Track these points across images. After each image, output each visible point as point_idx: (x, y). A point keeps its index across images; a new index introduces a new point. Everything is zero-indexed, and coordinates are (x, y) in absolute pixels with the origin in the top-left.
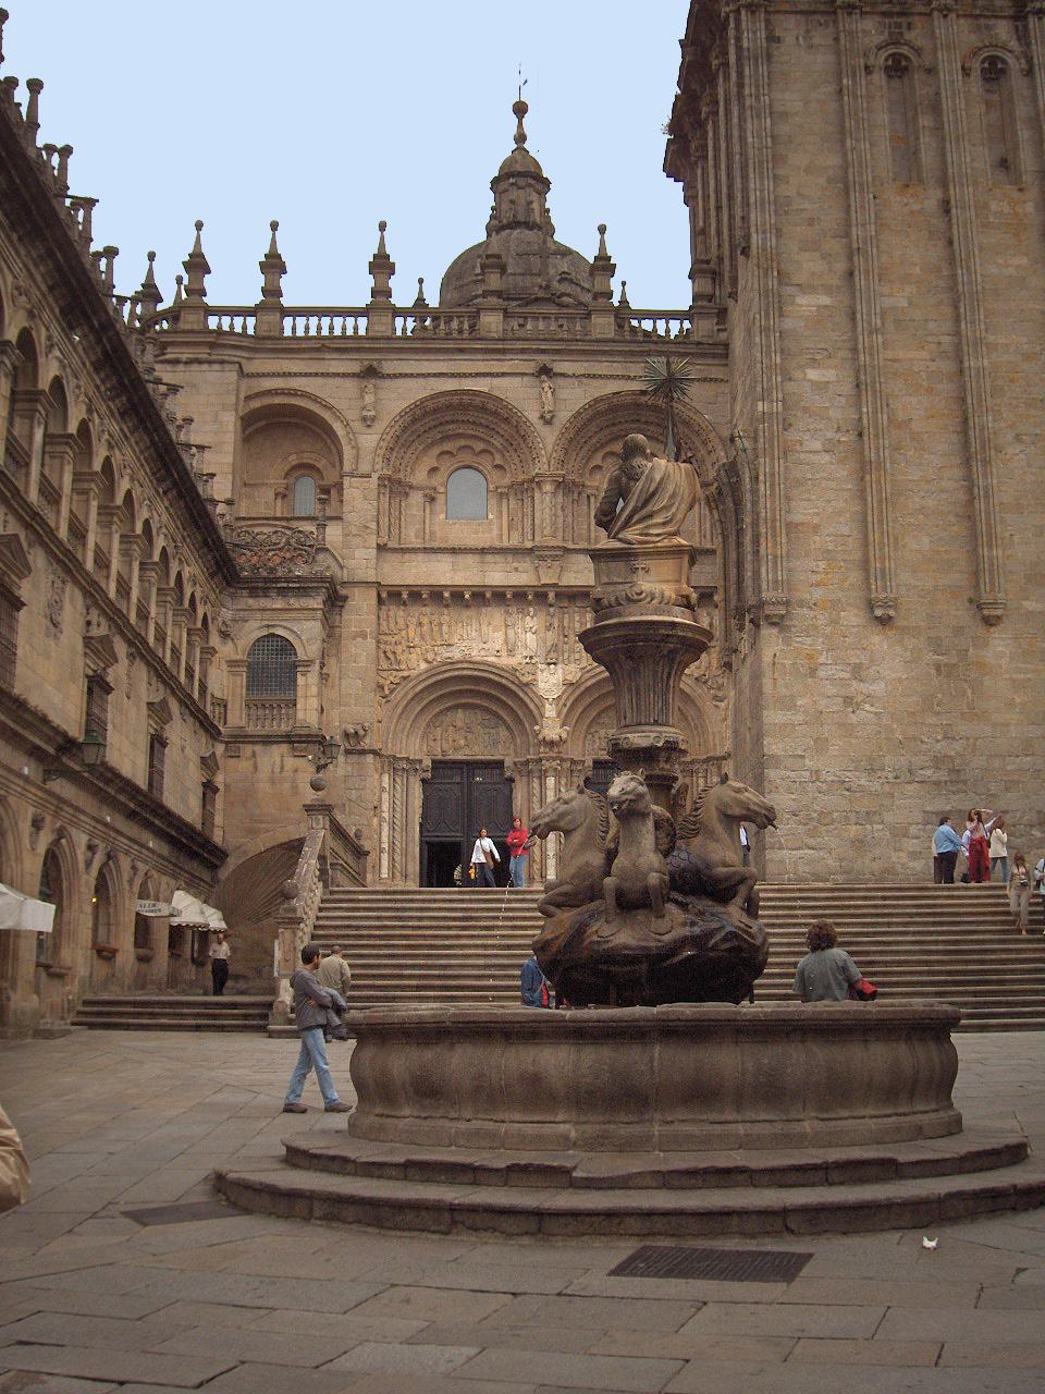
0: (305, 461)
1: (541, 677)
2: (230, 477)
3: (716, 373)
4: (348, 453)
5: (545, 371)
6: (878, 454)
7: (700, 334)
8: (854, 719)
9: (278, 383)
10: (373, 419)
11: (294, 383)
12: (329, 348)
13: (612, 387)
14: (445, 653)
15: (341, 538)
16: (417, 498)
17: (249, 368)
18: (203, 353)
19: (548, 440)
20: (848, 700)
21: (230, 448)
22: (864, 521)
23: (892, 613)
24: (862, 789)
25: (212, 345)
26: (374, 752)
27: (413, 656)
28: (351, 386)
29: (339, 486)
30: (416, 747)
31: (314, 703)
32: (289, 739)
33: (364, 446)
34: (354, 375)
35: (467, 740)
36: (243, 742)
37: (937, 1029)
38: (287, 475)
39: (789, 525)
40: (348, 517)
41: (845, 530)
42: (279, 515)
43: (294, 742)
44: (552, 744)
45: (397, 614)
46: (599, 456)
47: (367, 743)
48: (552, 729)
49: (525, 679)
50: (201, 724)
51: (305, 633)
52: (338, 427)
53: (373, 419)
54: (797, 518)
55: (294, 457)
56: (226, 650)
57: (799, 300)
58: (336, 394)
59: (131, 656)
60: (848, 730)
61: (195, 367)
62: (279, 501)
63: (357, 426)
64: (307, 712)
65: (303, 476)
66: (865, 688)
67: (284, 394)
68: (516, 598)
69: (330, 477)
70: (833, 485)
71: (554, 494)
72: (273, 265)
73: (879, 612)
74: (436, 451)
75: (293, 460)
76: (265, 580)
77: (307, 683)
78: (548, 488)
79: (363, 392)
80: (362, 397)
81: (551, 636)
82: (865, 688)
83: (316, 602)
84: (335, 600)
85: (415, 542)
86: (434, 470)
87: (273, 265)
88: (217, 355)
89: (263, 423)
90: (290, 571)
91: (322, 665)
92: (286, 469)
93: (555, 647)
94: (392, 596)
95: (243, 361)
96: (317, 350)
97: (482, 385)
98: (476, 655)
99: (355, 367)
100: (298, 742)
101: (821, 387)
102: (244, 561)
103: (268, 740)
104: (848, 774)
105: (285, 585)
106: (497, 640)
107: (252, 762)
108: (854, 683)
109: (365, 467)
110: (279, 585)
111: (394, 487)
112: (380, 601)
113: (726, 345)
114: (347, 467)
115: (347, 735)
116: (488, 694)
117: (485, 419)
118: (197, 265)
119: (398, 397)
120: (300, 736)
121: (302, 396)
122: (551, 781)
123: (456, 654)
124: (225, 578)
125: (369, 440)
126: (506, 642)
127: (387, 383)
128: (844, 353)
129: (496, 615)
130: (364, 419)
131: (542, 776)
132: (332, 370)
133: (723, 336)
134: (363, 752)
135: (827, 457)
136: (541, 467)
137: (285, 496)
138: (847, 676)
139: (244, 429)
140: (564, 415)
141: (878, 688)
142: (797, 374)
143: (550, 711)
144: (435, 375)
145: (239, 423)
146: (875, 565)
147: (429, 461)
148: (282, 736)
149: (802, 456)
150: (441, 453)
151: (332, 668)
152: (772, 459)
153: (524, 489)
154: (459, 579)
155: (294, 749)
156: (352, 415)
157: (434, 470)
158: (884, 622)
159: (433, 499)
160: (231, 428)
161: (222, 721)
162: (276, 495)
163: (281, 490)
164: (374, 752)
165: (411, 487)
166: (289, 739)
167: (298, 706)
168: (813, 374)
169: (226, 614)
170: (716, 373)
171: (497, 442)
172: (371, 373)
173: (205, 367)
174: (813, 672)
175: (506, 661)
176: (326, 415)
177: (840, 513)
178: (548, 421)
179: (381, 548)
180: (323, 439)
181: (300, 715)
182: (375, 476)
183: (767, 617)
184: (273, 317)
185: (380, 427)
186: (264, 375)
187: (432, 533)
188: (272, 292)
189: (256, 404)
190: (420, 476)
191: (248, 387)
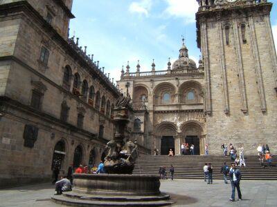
19: (177, 89)
30: (161, 134)
35: (167, 133)
45: (156, 115)
48: (179, 131)
51: (142, 118)
58: (148, 84)
59: (110, 122)
68: (173, 112)
72: (138, 66)
83: (144, 114)
84: (146, 113)
87: (138, 66)
94: (155, 112)
111: (156, 97)
116: (171, 126)
119: (157, 83)
125: (152, 90)
129: (171, 114)
136: (176, 92)
151: (147, 123)
153: (174, 96)
188: (138, 70)
190: (160, 95)
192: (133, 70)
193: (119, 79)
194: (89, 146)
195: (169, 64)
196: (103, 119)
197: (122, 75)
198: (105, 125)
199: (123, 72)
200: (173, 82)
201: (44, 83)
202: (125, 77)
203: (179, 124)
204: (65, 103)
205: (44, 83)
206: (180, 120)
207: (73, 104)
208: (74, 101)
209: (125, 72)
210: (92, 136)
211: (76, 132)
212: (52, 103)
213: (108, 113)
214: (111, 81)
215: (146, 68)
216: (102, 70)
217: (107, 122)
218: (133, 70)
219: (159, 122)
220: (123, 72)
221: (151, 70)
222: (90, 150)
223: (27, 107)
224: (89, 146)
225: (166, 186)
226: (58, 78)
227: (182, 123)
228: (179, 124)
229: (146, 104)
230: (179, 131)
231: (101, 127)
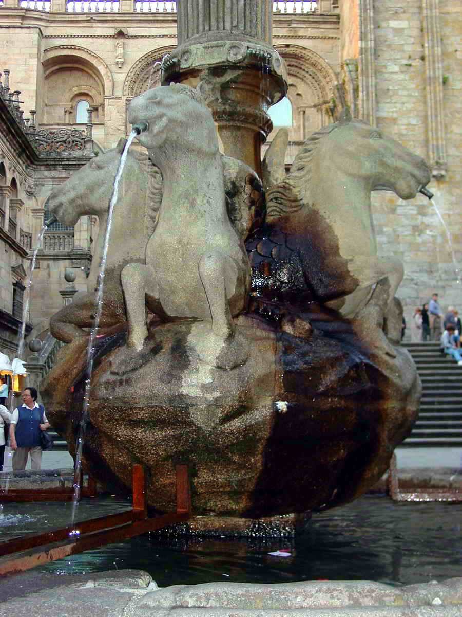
0: (83, 91)
2: (35, 98)
4: (108, 84)
6: (434, 73)
7: (323, 10)
8: (419, 240)
9: (64, 42)
10: (123, 64)
11: (74, 42)
12: (95, 20)
15: (103, 136)
17: (47, 32)
18: (17, 22)
21: (34, 80)
23: (443, 173)
24: (424, 284)
25: (23, 18)
28: (110, 43)
29: (103, 105)
31: (85, 235)
32: (70, 257)
36: (41, 259)
38: (72, 99)
39: (378, 119)
40: (108, 123)
41: (414, 122)
42: (67, 123)
43: (72, 259)
50: (10, 245)
52: (101, 69)
53: (123, 64)
54: (383, 114)
55: (75, 89)
56: (30, 204)
61: (11, 30)
62: (67, 115)
63: (114, 68)
65: (79, 101)
66: (427, 220)
67: (67, 48)
69: (98, 100)
70: (405, 93)
75: (76, 90)
76: (55, 159)
79: (116, 46)
80: (116, 50)
82: (427, 220)
88: (27, 23)
89: (57, 67)
90: (70, 154)
92: (72, 96)
95: (41, 28)
96: (88, 21)
99: (112, 32)
100: (75, 259)
101: (398, 31)
102: (42, 150)
103: (56, 258)
104: (415, 274)
105: (67, 163)
107: (47, 271)
108: (420, 217)
109: (118, 93)
110: (63, 163)
113: (338, 16)
114: (107, 93)
119: (138, 50)
120: (77, 255)
121: (79, 49)
124: (28, 157)
125: (121, 77)
127: (131, 41)
128: (416, 10)
130: (117, 63)
132: (97, 34)
133: (337, 11)
135: (402, 76)
137: (71, 112)
139: (45, 72)
142: (384, 24)
144: (160, 36)
145: (41, 66)
146: (432, 142)
148: (65, 255)
149: (386, 75)
152: (367, 77)
155: (73, 263)
156: (110, 61)
160: (35, 68)
161: (29, 247)
162: (65, 112)
163: (69, 109)
167: (75, 237)
168: (394, 24)
169: (31, 181)
170: (331, 33)
173: (18, 30)
174: (393, 211)
176: (94, 62)
177: (410, 111)
180: (93, 77)
181: (77, 243)
182: (125, 98)
185: (127, 68)
186: (55, 37)
189: (52, 54)
191: (45, 44)
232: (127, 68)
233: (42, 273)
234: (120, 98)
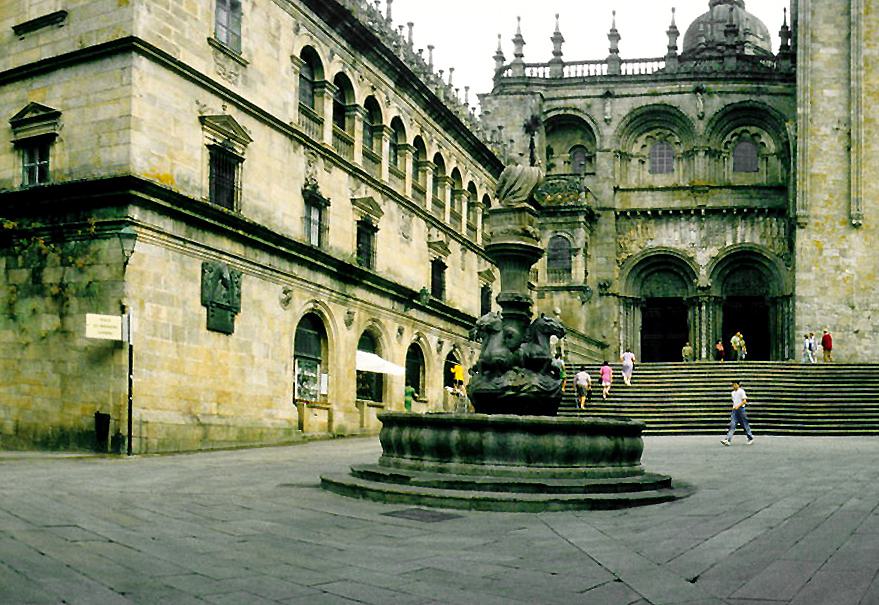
1: (698, 254)
3: (792, 84)
5: (698, 90)
13: (736, 99)
14: (650, 243)
16: (635, 161)
19: (701, 127)
20: (838, 268)
22: (850, 173)
23: (860, 222)
26: (614, 295)
27: (634, 246)
29: (595, 155)
32: (568, 289)
33: (607, 135)
34: (601, 97)
35: (665, 288)
37: (636, 432)
44: (703, 289)
46: (729, 136)
47: (610, 290)
48: (703, 278)
49: (691, 255)
53: (610, 120)
54: (815, 171)
57: (821, 51)
60: (835, 283)
64: (578, 275)
71: (705, 157)
73: (854, 222)
74: (645, 136)
77: (578, 261)
78: (702, 154)
81: (703, 234)
83: (582, 218)
84: (592, 218)
85: (633, 184)
86: (644, 146)
91: (585, 251)
93: (705, 239)
96: (581, 83)
97: (667, 99)
98: (665, 243)
99: (600, 92)
103: (557, 289)
106: (676, 236)
112: (617, 217)
115: (600, 286)
117: (668, 118)
118: (519, 41)
119: (621, 108)
122: (704, 308)
123: (654, 244)
125: (609, 131)
126: (681, 236)
130: (606, 120)
131: (700, 306)
134: (608, 295)
138: (838, 255)
140: (709, 113)
141: (852, 262)
143: (703, 272)
146: (854, 195)
147: (642, 140)
150: (648, 137)
154: (656, 205)
157: (644, 146)
158: (857, 226)
159: (643, 162)
164: (614, 295)
165: (632, 156)
166: (568, 289)
171: (676, 130)
172: (608, 95)
175: (681, 247)
178: (701, 118)
179: (616, 189)
182: (611, 154)
183: (799, 224)
184: (559, 67)
185: (614, 124)
187: (644, 180)
192: (538, 52)
193: (488, 86)
194: (400, 331)
195: (673, 32)
196: (442, 237)
197: (500, 72)
198: (447, 261)
199: (500, 57)
200: (689, 104)
201: (242, 119)
202: (509, 82)
203: (703, 259)
204: (315, 187)
205: (242, 119)
206: (705, 242)
207: (336, 185)
208: (340, 176)
209: (510, 59)
210: (405, 297)
211: (357, 284)
212: (271, 186)
213: (456, 217)
214: (461, 97)
215: (586, 49)
216: (425, 55)
217: (455, 246)
218: (538, 52)
219: (634, 249)
220: (500, 57)
221: (606, 54)
222: (408, 339)
223: (340, 265)
224: (400, 331)
225: (659, 453)
226: (279, 93)
227: (714, 251)
228: (703, 259)
229: (588, 182)
230: (703, 278)
231: (438, 268)
232: (614, 124)
233: (546, 302)
234: (608, 151)
